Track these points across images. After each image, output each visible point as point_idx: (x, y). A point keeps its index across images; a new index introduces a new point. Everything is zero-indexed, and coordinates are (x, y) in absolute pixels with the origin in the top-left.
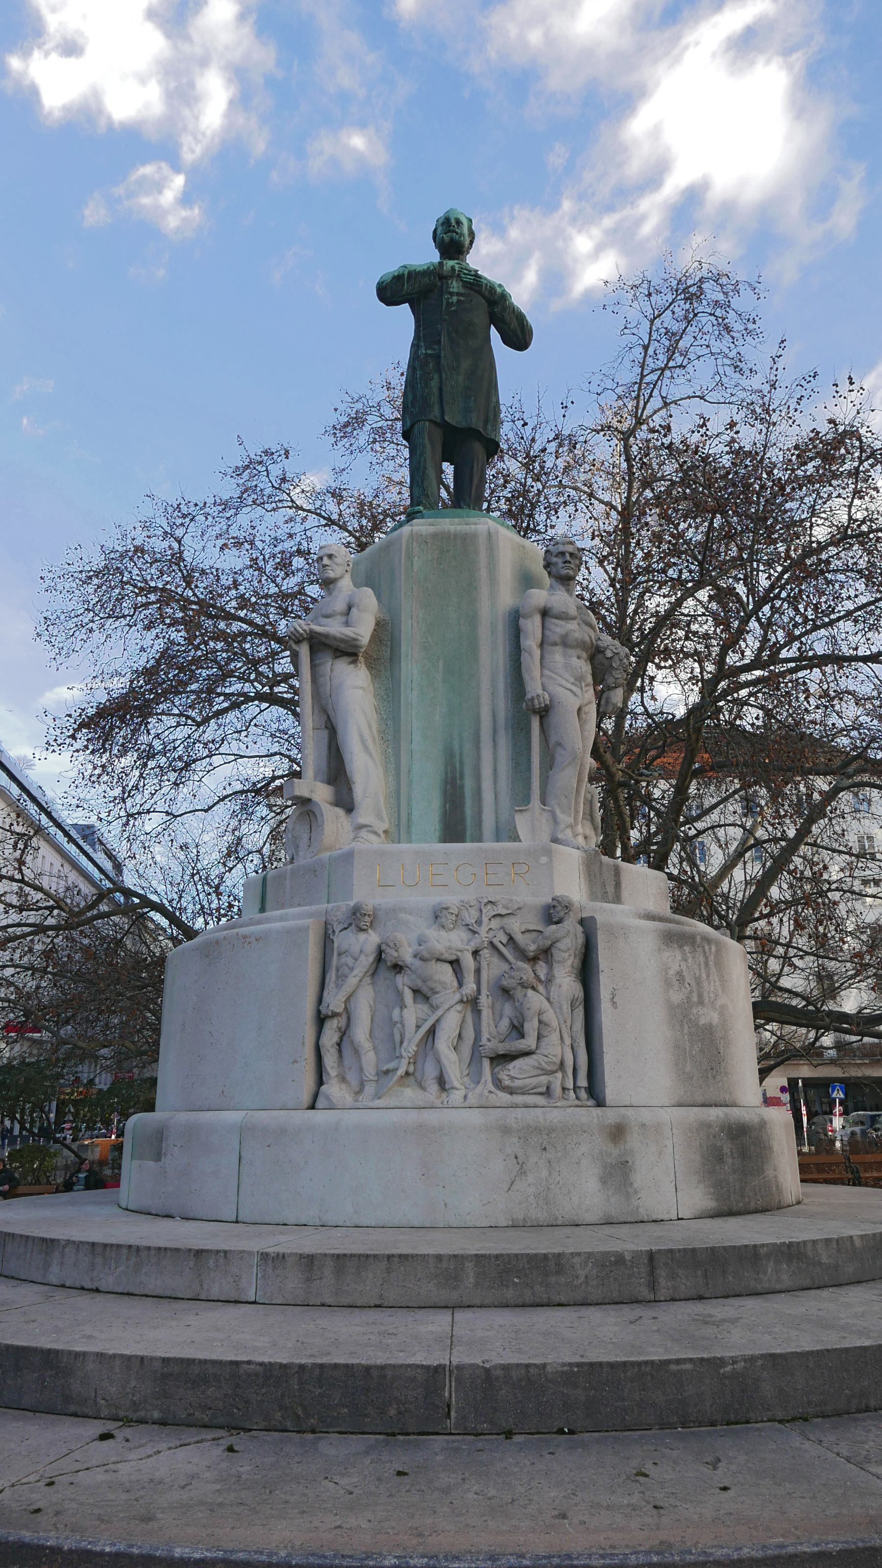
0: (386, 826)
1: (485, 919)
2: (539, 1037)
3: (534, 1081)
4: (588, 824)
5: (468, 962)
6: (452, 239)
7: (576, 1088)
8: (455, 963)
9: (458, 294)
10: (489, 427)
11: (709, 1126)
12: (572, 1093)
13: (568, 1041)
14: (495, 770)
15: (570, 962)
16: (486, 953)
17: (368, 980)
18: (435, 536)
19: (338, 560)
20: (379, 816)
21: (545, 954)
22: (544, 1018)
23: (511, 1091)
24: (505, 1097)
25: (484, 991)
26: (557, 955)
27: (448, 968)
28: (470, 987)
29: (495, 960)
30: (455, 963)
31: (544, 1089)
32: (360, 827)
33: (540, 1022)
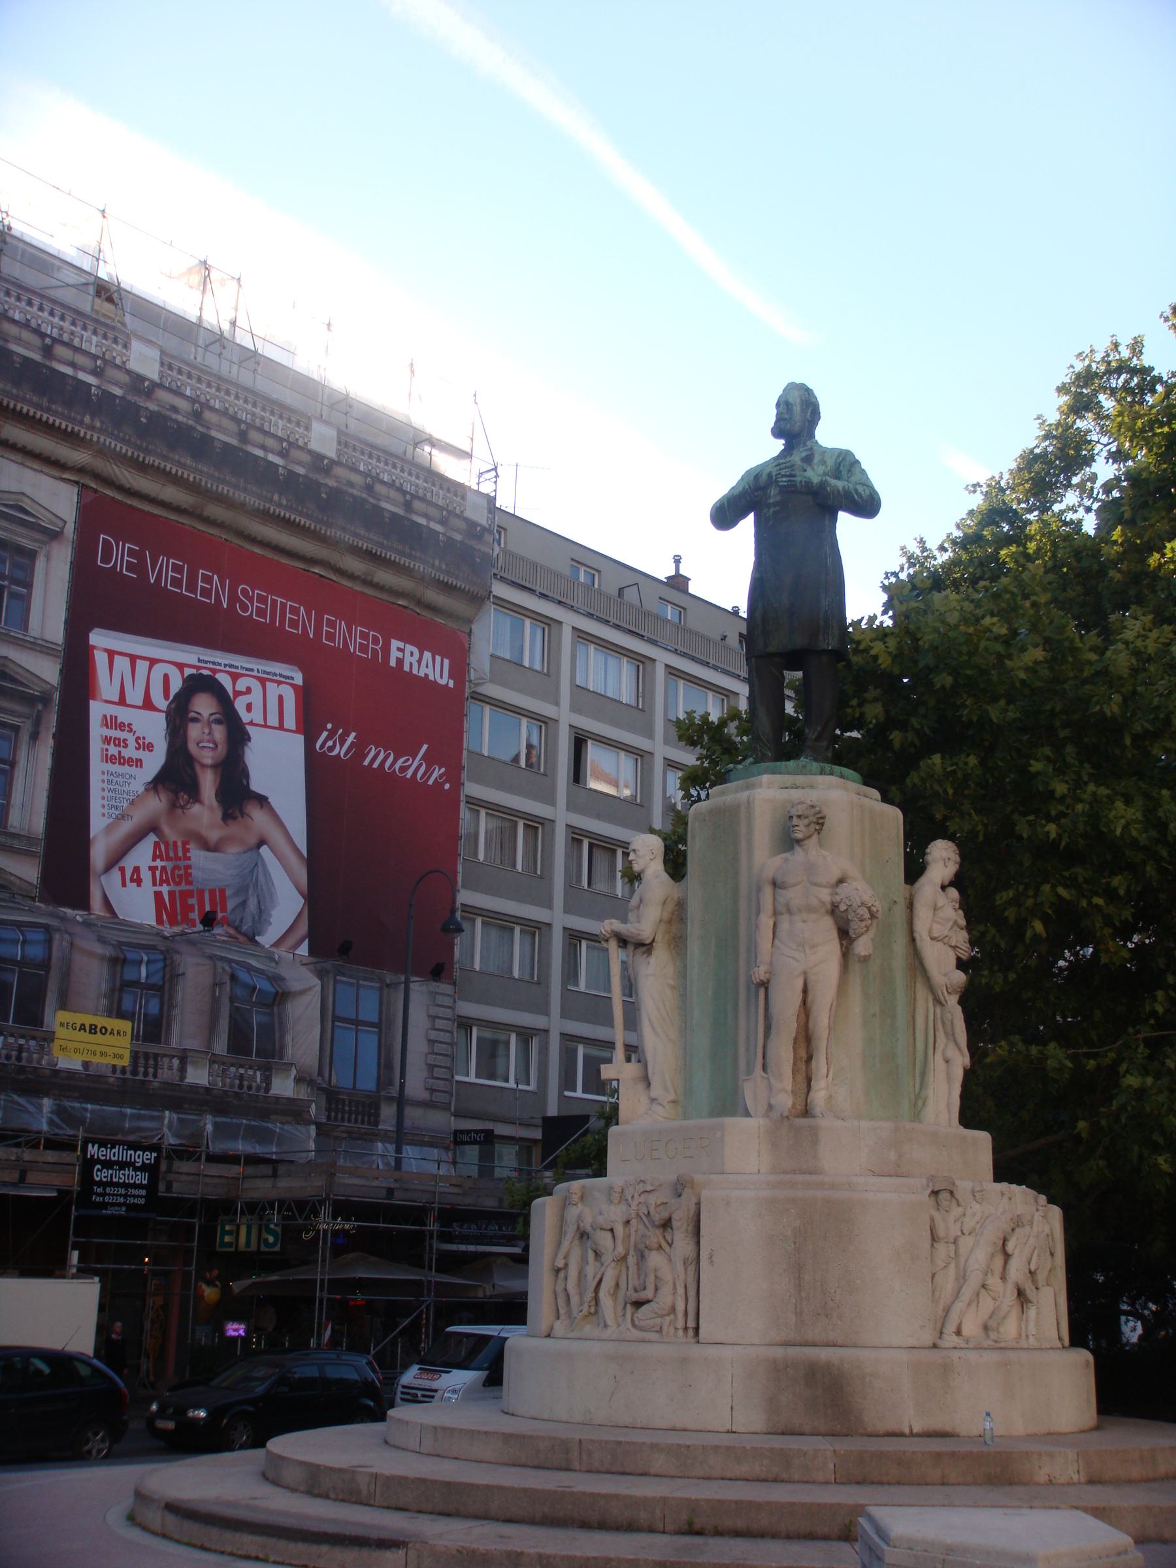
0: (672, 1096)
1: (636, 1195)
2: (656, 1289)
3: (651, 1322)
4: (951, 1046)
5: (620, 1230)
6: (797, 416)
7: (686, 1329)
8: (612, 1230)
9: (775, 504)
10: (821, 638)
11: (775, 1361)
12: (681, 1332)
13: (681, 1291)
14: (748, 1037)
15: (684, 1229)
16: (634, 1222)
17: (576, 1242)
18: (710, 812)
19: (640, 853)
20: (666, 1089)
21: (667, 1224)
22: (658, 1274)
23: (641, 1329)
24: (636, 1334)
25: (632, 1252)
26: (675, 1224)
27: (609, 1234)
28: (620, 1250)
29: (641, 1227)
30: (612, 1230)
31: (658, 1328)
32: (653, 1100)
33: (656, 1277)
